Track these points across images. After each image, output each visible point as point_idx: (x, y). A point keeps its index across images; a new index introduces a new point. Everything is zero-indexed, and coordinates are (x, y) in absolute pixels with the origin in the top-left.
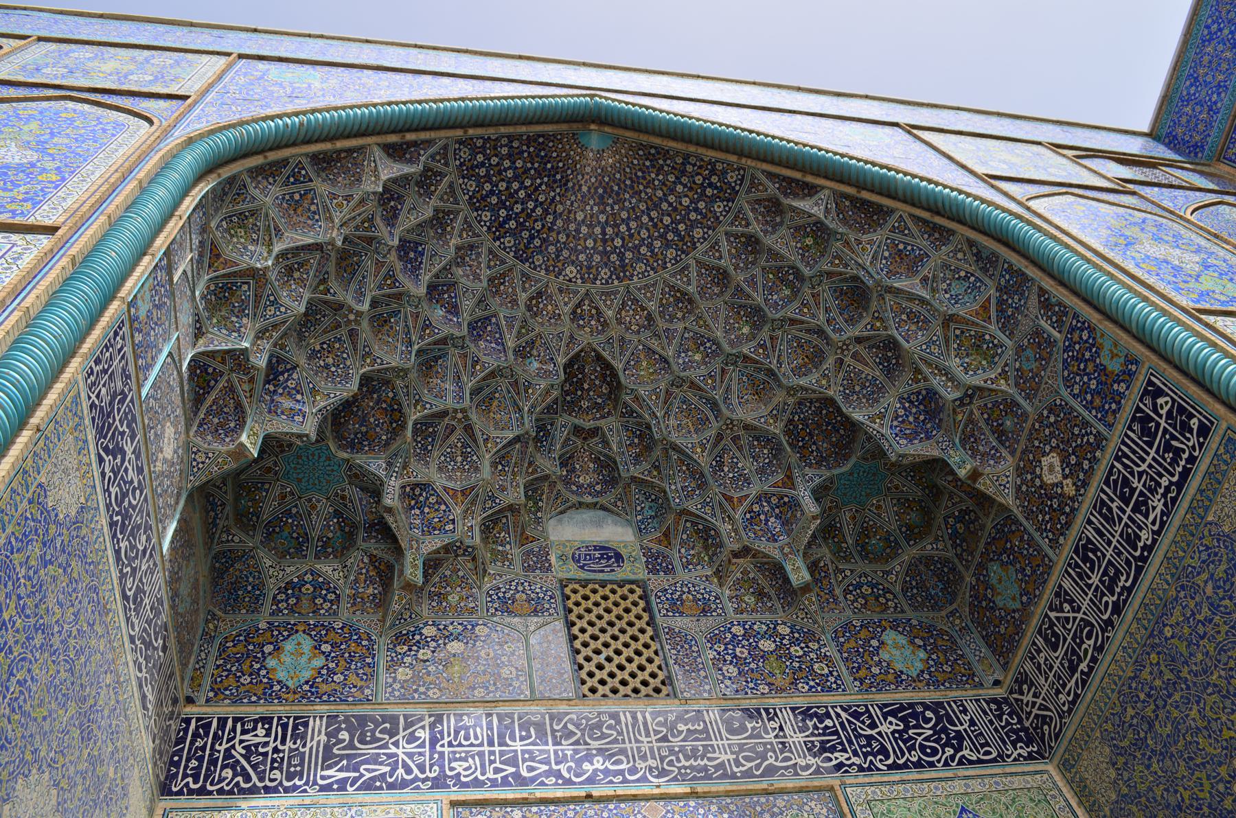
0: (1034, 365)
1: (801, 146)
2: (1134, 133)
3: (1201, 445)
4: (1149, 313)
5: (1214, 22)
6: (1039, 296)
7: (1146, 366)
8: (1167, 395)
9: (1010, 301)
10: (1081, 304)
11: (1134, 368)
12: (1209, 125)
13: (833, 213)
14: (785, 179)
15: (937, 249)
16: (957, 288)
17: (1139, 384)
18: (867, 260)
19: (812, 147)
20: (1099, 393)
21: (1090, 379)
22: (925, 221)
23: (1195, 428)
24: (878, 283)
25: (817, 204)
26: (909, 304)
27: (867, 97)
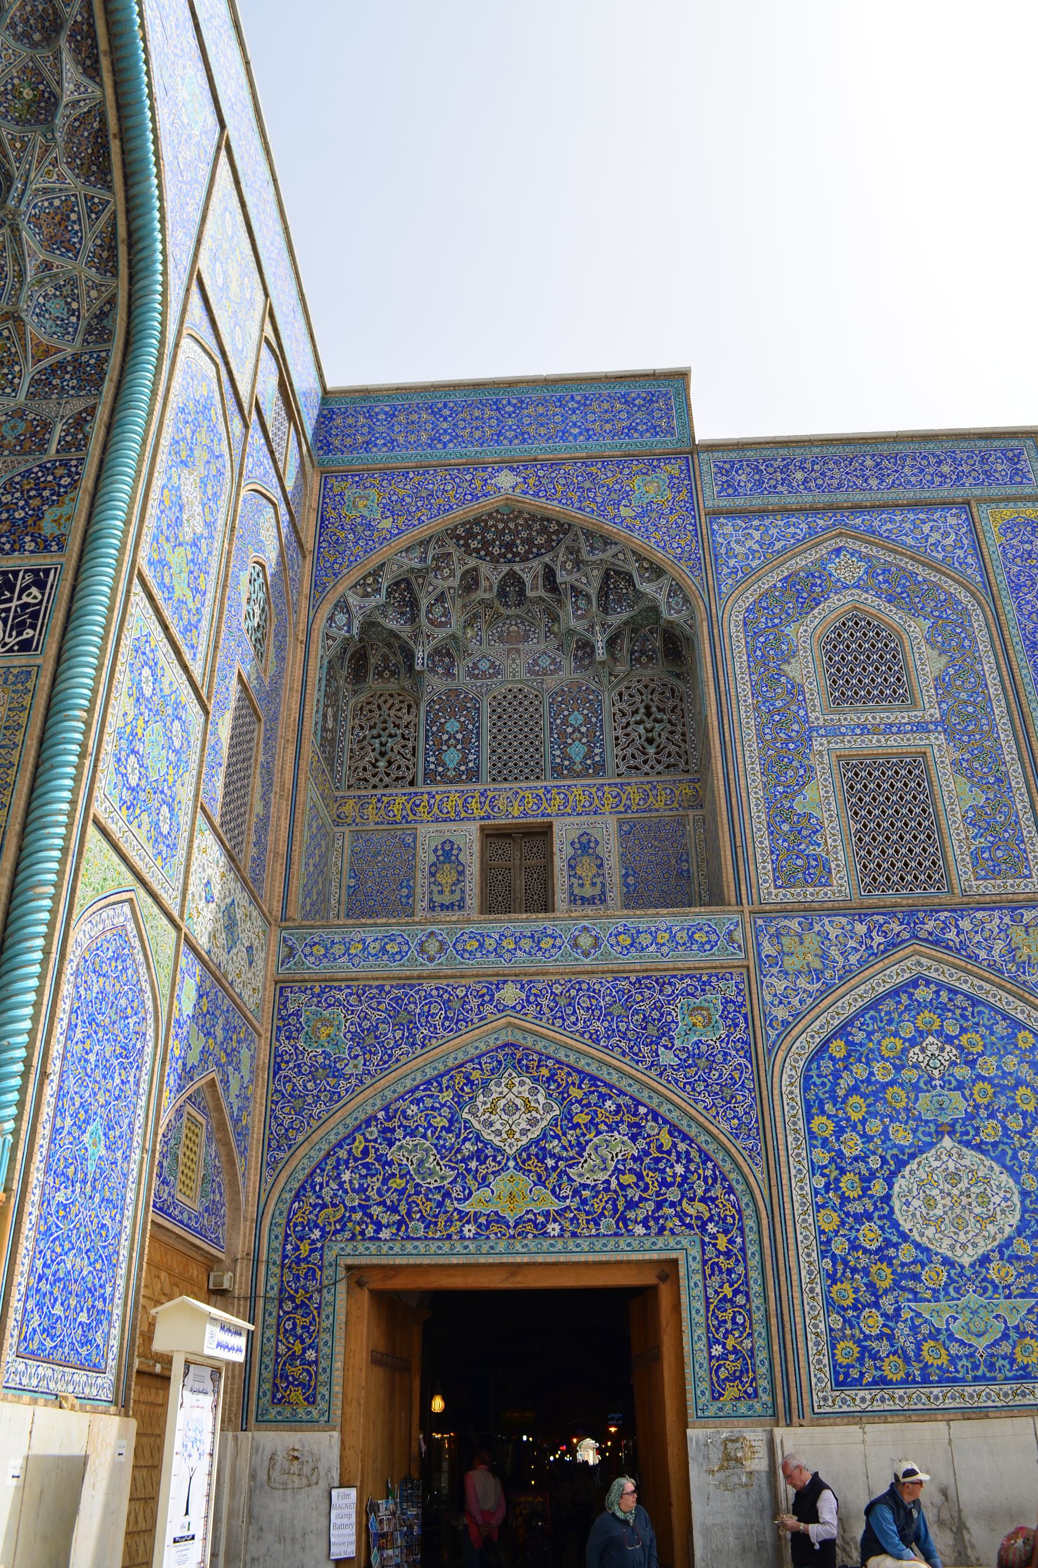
0: (10, 439)
1: (140, 34)
2: (321, 376)
3: (11, 650)
4: (114, 536)
5: (451, 409)
6: (85, 410)
7: (63, 560)
8: (43, 594)
9: (67, 377)
10: (96, 461)
11: (54, 548)
12: (353, 448)
13: (76, 113)
14: (92, 26)
15: (90, 264)
16: (56, 307)
17: (41, 561)
18: (38, 183)
19: (145, 50)
20: (13, 525)
21: (23, 508)
22: (114, 234)
23: (25, 636)
24: (15, 213)
25: (78, 86)
26: (10, 261)
27: (247, 63)
